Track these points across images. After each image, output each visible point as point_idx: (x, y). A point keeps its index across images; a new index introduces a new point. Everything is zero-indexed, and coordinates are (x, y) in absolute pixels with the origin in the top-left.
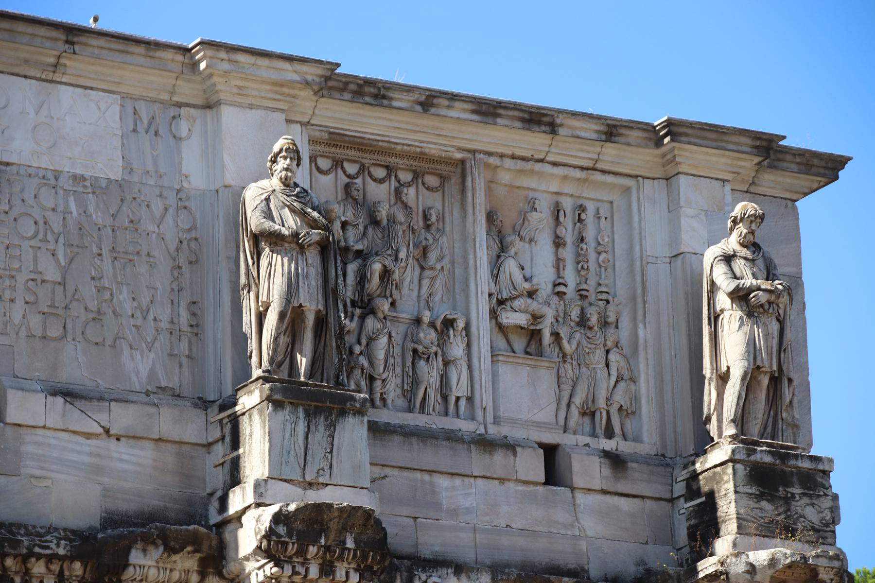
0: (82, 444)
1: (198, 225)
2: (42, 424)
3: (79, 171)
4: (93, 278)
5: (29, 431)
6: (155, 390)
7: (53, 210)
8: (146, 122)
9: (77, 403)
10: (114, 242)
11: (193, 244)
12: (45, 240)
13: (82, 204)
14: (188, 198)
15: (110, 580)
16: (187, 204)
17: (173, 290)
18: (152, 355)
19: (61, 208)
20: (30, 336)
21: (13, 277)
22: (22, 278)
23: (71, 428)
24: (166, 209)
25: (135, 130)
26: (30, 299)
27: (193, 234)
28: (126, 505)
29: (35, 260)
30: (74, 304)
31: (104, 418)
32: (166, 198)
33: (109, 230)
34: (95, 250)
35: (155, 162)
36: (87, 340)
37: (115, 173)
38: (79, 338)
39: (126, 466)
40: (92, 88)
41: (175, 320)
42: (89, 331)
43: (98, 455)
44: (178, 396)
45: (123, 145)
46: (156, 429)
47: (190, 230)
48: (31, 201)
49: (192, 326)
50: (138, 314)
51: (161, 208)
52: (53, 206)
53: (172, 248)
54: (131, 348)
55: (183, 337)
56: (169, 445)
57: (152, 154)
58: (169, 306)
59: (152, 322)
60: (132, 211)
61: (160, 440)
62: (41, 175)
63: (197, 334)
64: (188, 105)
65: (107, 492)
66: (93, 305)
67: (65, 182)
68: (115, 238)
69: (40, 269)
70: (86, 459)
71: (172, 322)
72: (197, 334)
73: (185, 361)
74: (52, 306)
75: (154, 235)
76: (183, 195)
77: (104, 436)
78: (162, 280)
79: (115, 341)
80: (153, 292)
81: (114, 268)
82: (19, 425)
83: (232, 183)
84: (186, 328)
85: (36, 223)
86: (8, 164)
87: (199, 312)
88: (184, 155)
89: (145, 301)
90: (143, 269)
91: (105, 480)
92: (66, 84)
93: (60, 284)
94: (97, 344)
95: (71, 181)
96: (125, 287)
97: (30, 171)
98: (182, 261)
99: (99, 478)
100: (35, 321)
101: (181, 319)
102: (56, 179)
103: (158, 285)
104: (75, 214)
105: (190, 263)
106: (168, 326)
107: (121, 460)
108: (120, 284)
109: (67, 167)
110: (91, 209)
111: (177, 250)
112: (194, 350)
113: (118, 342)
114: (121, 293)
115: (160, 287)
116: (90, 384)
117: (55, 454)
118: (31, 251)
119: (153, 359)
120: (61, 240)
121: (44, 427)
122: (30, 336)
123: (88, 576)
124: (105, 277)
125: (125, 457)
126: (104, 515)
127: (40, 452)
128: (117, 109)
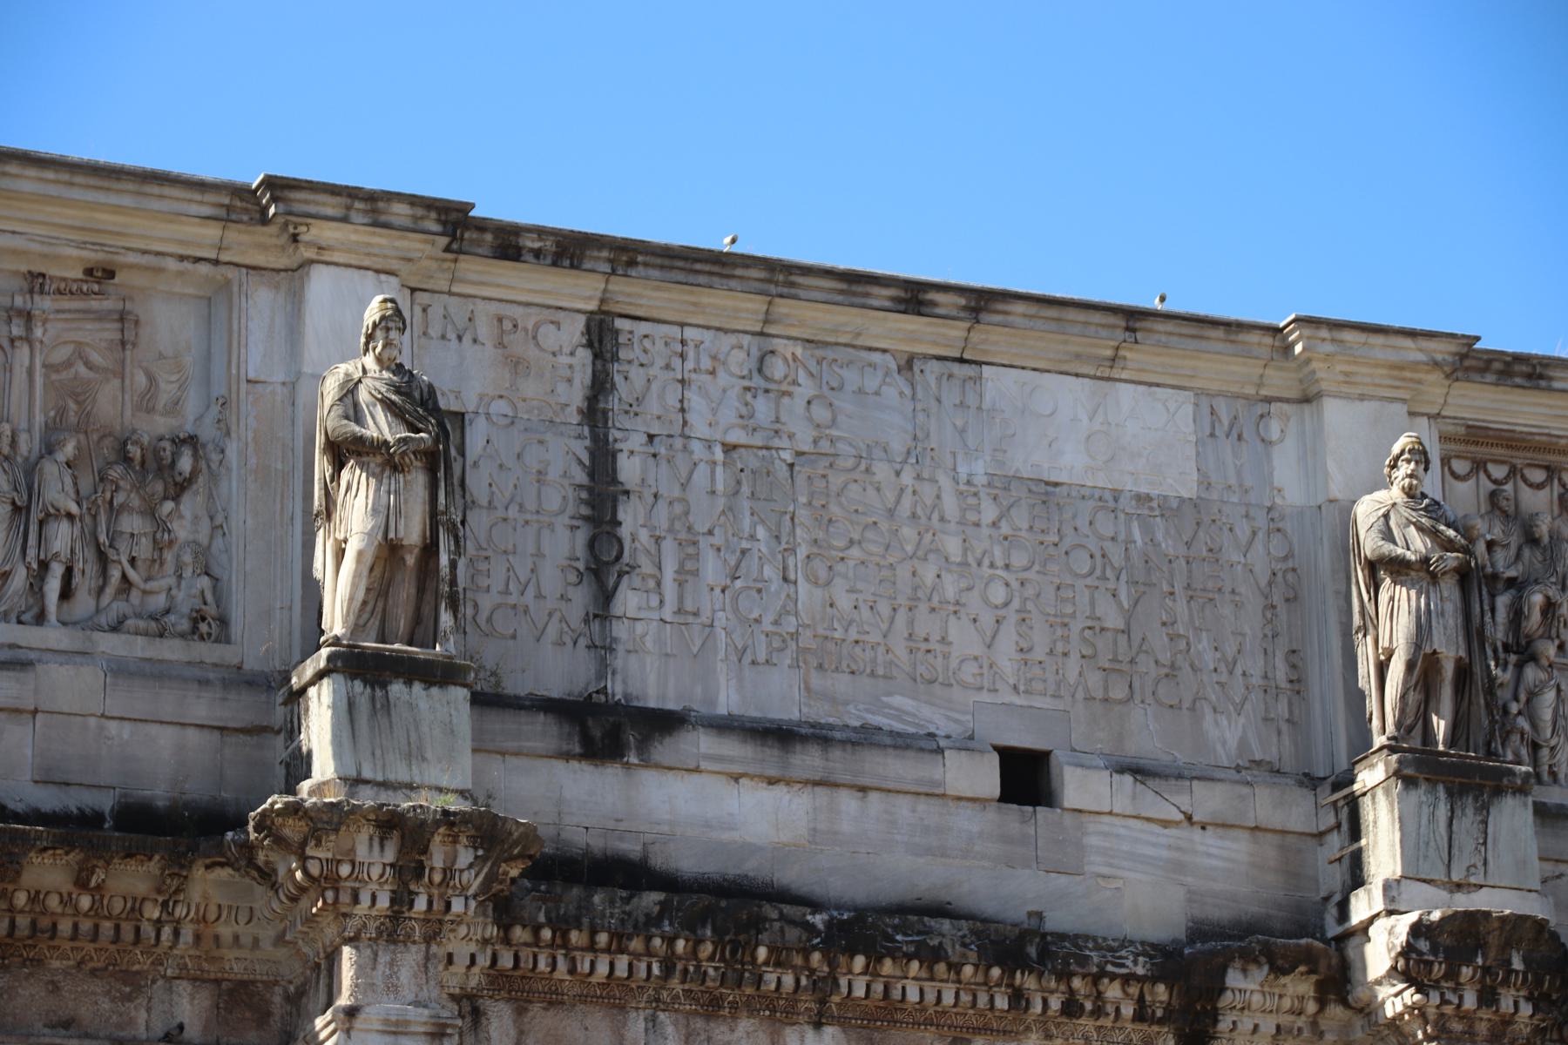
0: (1158, 835)
1: (1296, 552)
2: (1108, 810)
3: (1144, 490)
4: (1164, 624)
5: (1092, 818)
6: (1247, 765)
7: (1113, 539)
8: (1226, 423)
9: (1150, 782)
10: (1190, 577)
11: (1290, 576)
12: (1104, 578)
13: (1147, 530)
14: (1282, 518)
15: (1203, 1007)
16: (1280, 525)
17: (1265, 636)
18: (1242, 720)
19: (1122, 537)
20: (1089, 699)
21: (1066, 625)
22: (1076, 627)
23: (1143, 815)
24: (1254, 533)
25: (1212, 435)
26: (1087, 651)
27: (1290, 564)
28: (1218, 912)
29: (1092, 603)
30: (1142, 658)
31: (1184, 801)
32: (1254, 519)
33: (1183, 563)
34: (1166, 588)
35: (1239, 473)
36: (1159, 703)
37: (1189, 490)
38: (1150, 700)
39: (1214, 862)
40: (1158, 385)
41: (1269, 675)
42: (1161, 691)
43: (1178, 849)
44: (1278, 771)
45: (1198, 454)
46: (1251, 814)
47: (1285, 558)
48: (1085, 529)
49: (1291, 681)
50: (1222, 668)
51: (1248, 532)
52: (1112, 534)
53: (1263, 582)
54: (1215, 711)
55: (1280, 696)
56: (1269, 836)
57: (1236, 465)
58: (1262, 656)
59: (1240, 678)
60: (1211, 538)
61: (1256, 828)
62: (1097, 496)
63: (1298, 692)
64: (1280, 400)
65: (1192, 896)
66: (1166, 658)
67: (1126, 504)
68: (1190, 571)
69: (1098, 615)
70: (1165, 853)
71: (1266, 677)
72: (1298, 692)
73: (1285, 727)
74: (1115, 660)
75: (1239, 567)
76: (1275, 514)
77: (1186, 824)
78: (1251, 624)
79: (1194, 702)
80: (1240, 638)
81: (1190, 609)
82: (1080, 811)
83: (1339, 496)
84: (1284, 684)
85: (1092, 556)
86: (1056, 484)
87: (1300, 664)
88: (1276, 462)
89: (1230, 650)
90: (1227, 610)
91: (1189, 880)
92: (1126, 381)
93: (1123, 632)
94: (1171, 706)
95: (1134, 502)
96: (1204, 634)
97: (1084, 491)
98: (1277, 599)
99: (1182, 878)
100: (1094, 680)
101: (1278, 673)
102: (1116, 500)
103: (1247, 630)
104: (1139, 542)
105: (1287, 600)
106: (1261, 682)
107: (1209, 855)
108: (1198, 630)
109: (1128, 485)
110: (1159, 536)
111: (1270, 584)
112: (1296, 712)
113: (1198, 704)
114: (1200, 641)
115: (1249, 632)
116: (1166, 759)
117: (1125, 847)
118: (1087, 592)
119: (1244, 726)
120: (1124, 577)
121: (1110, 813)
122: (1089, 699)
123: (1175, 1002)
124: (1179, 620)
125: (1213, 851)
126: (1190, 924)
127: (1107, 845)
128: (1190, 409)
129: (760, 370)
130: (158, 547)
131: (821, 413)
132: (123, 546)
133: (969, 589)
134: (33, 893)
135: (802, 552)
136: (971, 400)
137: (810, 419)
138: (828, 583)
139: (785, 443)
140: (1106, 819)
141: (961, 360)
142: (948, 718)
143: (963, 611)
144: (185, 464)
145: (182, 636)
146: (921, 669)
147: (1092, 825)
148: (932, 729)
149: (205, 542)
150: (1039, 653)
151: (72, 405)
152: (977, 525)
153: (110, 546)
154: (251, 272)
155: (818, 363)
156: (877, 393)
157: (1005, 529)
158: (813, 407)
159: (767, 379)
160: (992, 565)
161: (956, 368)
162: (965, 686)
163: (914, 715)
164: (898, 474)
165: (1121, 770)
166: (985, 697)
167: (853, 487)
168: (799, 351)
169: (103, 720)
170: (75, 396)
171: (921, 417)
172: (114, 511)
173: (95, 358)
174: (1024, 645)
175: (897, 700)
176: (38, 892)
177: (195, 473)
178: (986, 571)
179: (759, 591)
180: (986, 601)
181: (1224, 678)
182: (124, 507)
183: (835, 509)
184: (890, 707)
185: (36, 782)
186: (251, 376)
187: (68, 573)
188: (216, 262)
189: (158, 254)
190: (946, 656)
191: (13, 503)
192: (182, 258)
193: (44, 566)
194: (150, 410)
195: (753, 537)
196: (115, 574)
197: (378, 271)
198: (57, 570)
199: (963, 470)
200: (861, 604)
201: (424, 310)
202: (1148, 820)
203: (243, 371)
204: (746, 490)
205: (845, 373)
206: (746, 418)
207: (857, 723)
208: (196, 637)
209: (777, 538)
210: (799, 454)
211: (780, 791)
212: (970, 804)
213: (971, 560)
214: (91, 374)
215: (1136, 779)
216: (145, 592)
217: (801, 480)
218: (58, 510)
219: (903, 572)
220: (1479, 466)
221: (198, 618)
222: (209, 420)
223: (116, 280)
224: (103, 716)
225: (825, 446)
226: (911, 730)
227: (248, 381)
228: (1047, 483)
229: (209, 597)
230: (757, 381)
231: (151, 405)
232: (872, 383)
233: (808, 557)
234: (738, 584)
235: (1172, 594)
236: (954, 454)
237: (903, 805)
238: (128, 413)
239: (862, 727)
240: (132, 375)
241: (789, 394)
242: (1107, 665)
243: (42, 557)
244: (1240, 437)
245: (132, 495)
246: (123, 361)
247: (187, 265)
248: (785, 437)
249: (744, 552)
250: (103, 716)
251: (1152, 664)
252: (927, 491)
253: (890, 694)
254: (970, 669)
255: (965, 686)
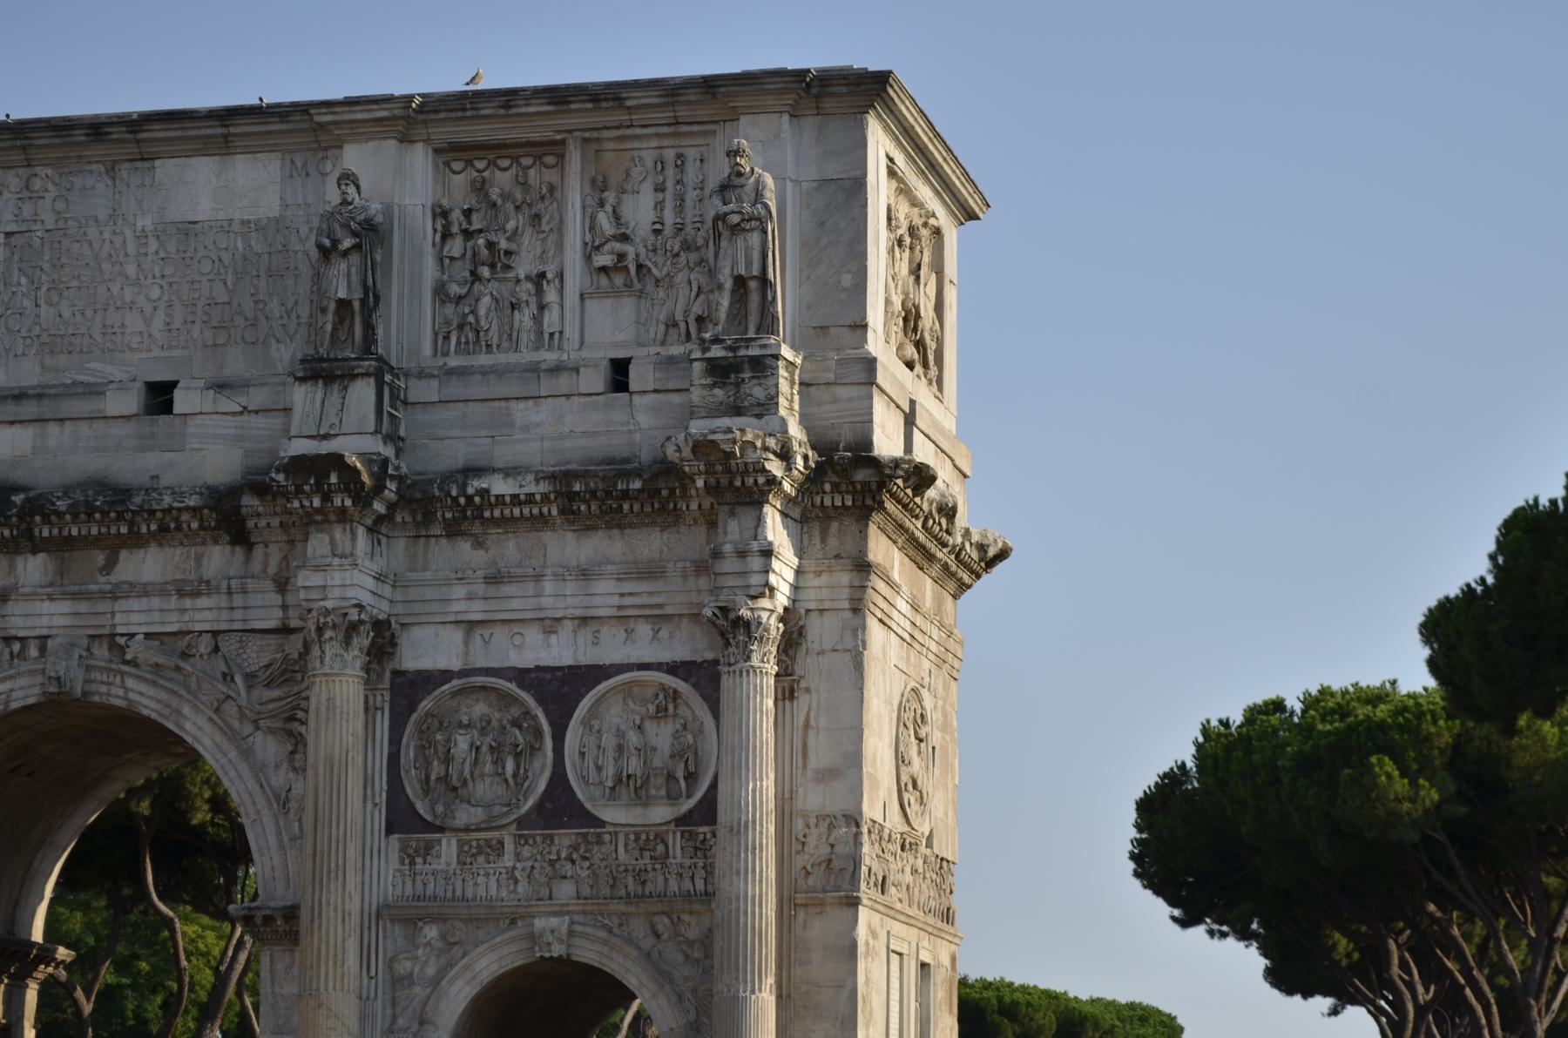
4: (252, 295)
7: (226, 249)
9: (224, 393)
18: (294, 345)
21: (195, 305)
22: (200, 305)
24: (311, 230)
25: (291, 176)
26: (206, 319)
29: (211, 290)
31: (243, 400)
33: (266, 256)
34: (255, 273)
37: (275, 212)
38: (240, 341)
42: (247, 338)
43: (241, 427)
50: (285, 315)
66: (250, 315)
70: (233, 431)
77: (246, 413)
79: (265, 340)
82: (185, 415)
91: (247, 445)
96: (275, 298)
102: (230, 225)
103: (302, 291)
107: (259, 428)
109: (237, 216)
110: (253, 243)
118: (208, 283)
125: (261, 426)
128: (278, 163)
129: (27, 188)
131: (60, 205)
133: (138, 293)
135: (44, 288)
136: (148, 182)
137: (54, 211)
138: (58, 303)
139: (39, 226)
140: (199, 417)
141: (143, 159)
142: (122, 370)
143: (134, 307)
146: (109, 345)
147: (191, 421)
148: (112, 378)
150: (177, 324)
152: (146, 254)
155: (61, 176)
156: (93, 188)
157: (162, 254)
158: (56, 203)
159: (32, 192)
160: (154, 277)
161: (139, 164)
162: (132, 350)
163: (102, 372)
164: (101, 233)
165: (208, 389)
166: (144, 355)
167: (76, 245)
168: (49, 172)
171: (117, 196)
174: (168, 320)
175: (93, 365)
178: (150, 281)
179: (21, 314)
180: (148, 299)
181: (285, 321)
183: (64, 260)
184: (88, 369)
190: (123, 334)
195: (19, 284)
199: (139, 224)
200: (76, 313)
202: (226, 413)
204: (16, 258)
205: (74, 180)
206: (18, 218)
207: (69, 382)
209: (33, 282)
210: (47, 231)
211: (17, 429)
212: (121, 420)
213: (141, 276)
215: (215, 391)
217: (46, 247)
219: (102, 290)
220: (469, 163)
225: (61, 224)
226: (100, 381)
228: (190, 223)
230: (26, 194)
232: (89, 183)
233: (48, 290)
234: (9, 312)
235: (258, 276)
236: (135, 215)
237: (84, 428)
239: (73, 383)
241: (43, 197)
242: (217, 325)
244: (308, 175)
248: (39, 223)
249: (14, 293)
251: (242, 319)
252: (118, 240)
253: (88, 362)
254: (136, 340)
255: (132, 350)
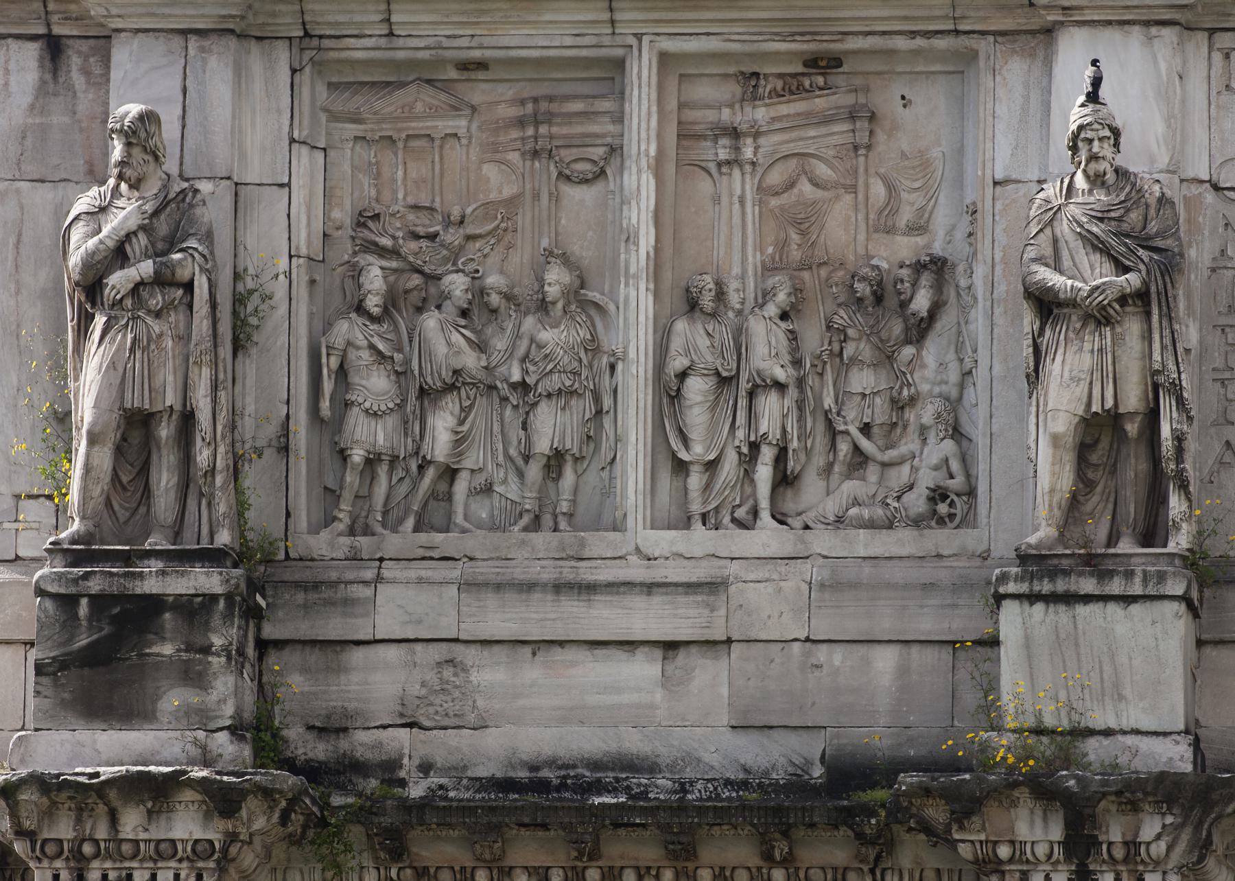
130: (898, 406)
132: (851, 413)
134: (717, 870)
144: (921, 302)
145: (917, 523)
149: (954, 393)
151: (795, 237)
153: (838, 414)
154: (999, 39)
169: (808, 645)
170: (797, 223)
172: (844, 365)
173: (823, 171)
176: (722, 869)
177: (936, 309)
182: (854, 360)
185: (733, 727)
186: (999, 176)
187: (782, 455)
188: (957, 32)
189: (884, 33)
191: (718, 374)
192: (913, 34)
193: (755, 447)
194: (890, 230)
196: (844, 447)
197: (1147, 23)
198: (767, 454)
201: (1227, 56)
203: (988, 172)
208: (933, 523)
214: (820, 194)
216: (885, 465)
218: (764, 381)
221: (938, 495)
222: (960, 234)
223: (845, 68)
224: (807, 640)
227: (996, 183)
229: (955, 466)
231: (890, 223)
238: (862, 237)
240: (867, 186)
243: (752, 438)
245: (862, 346)
246: (856, 171)
247: (920, 42)
250: (807, 640)
